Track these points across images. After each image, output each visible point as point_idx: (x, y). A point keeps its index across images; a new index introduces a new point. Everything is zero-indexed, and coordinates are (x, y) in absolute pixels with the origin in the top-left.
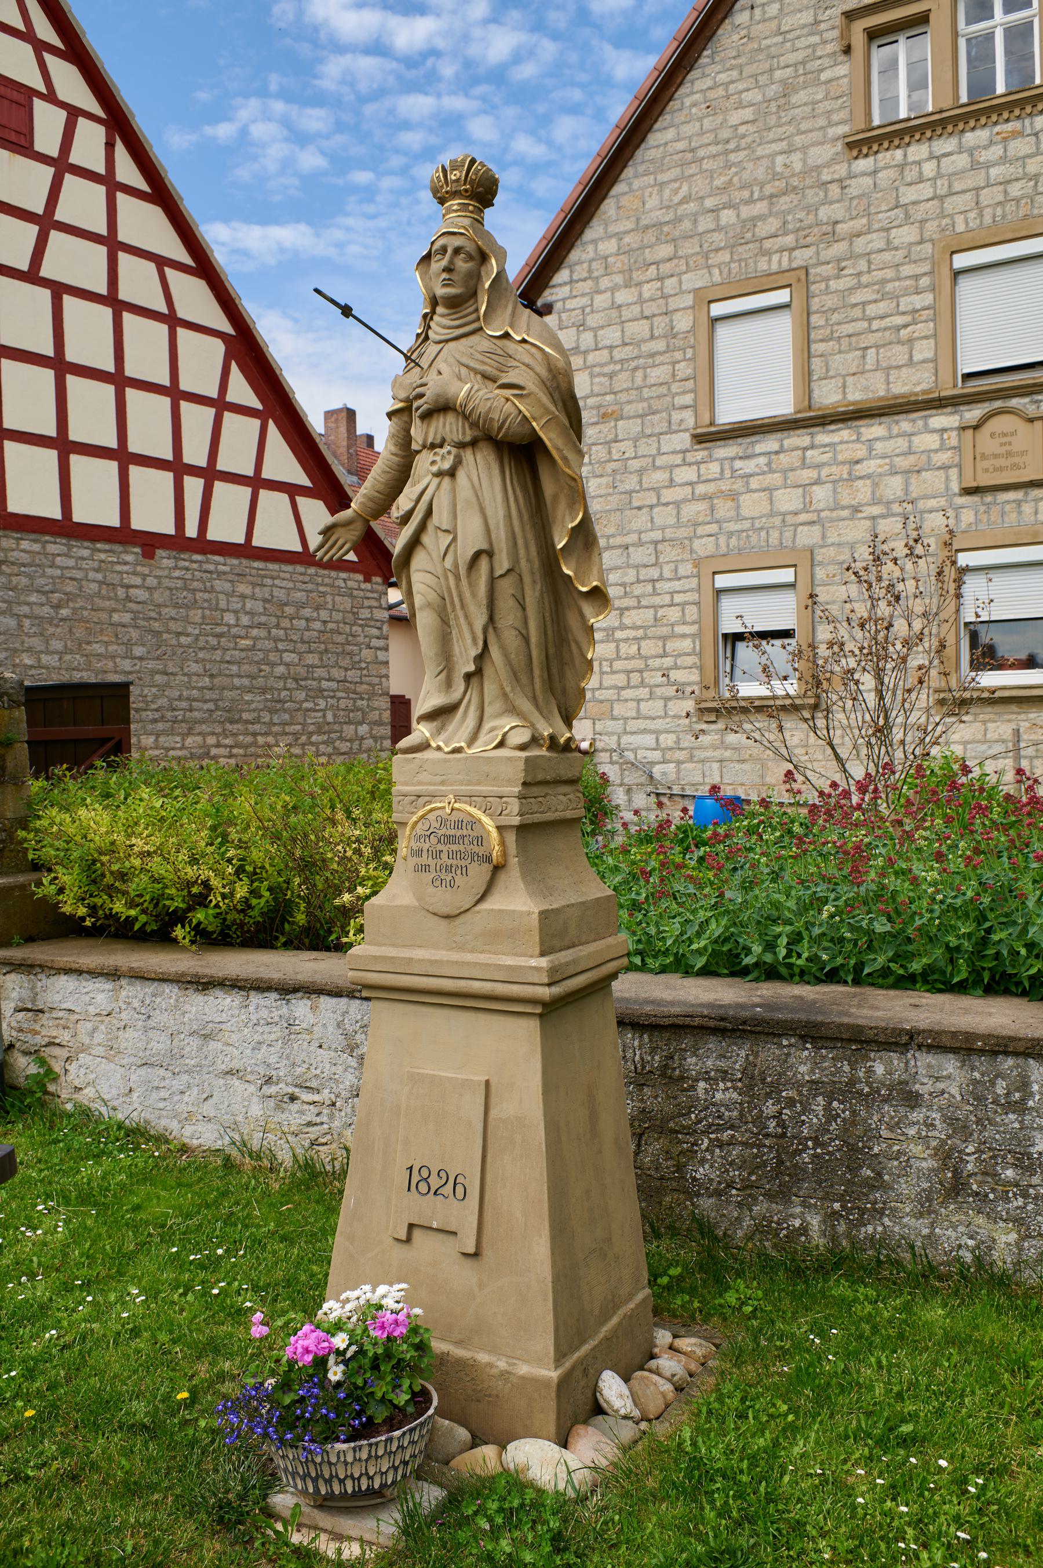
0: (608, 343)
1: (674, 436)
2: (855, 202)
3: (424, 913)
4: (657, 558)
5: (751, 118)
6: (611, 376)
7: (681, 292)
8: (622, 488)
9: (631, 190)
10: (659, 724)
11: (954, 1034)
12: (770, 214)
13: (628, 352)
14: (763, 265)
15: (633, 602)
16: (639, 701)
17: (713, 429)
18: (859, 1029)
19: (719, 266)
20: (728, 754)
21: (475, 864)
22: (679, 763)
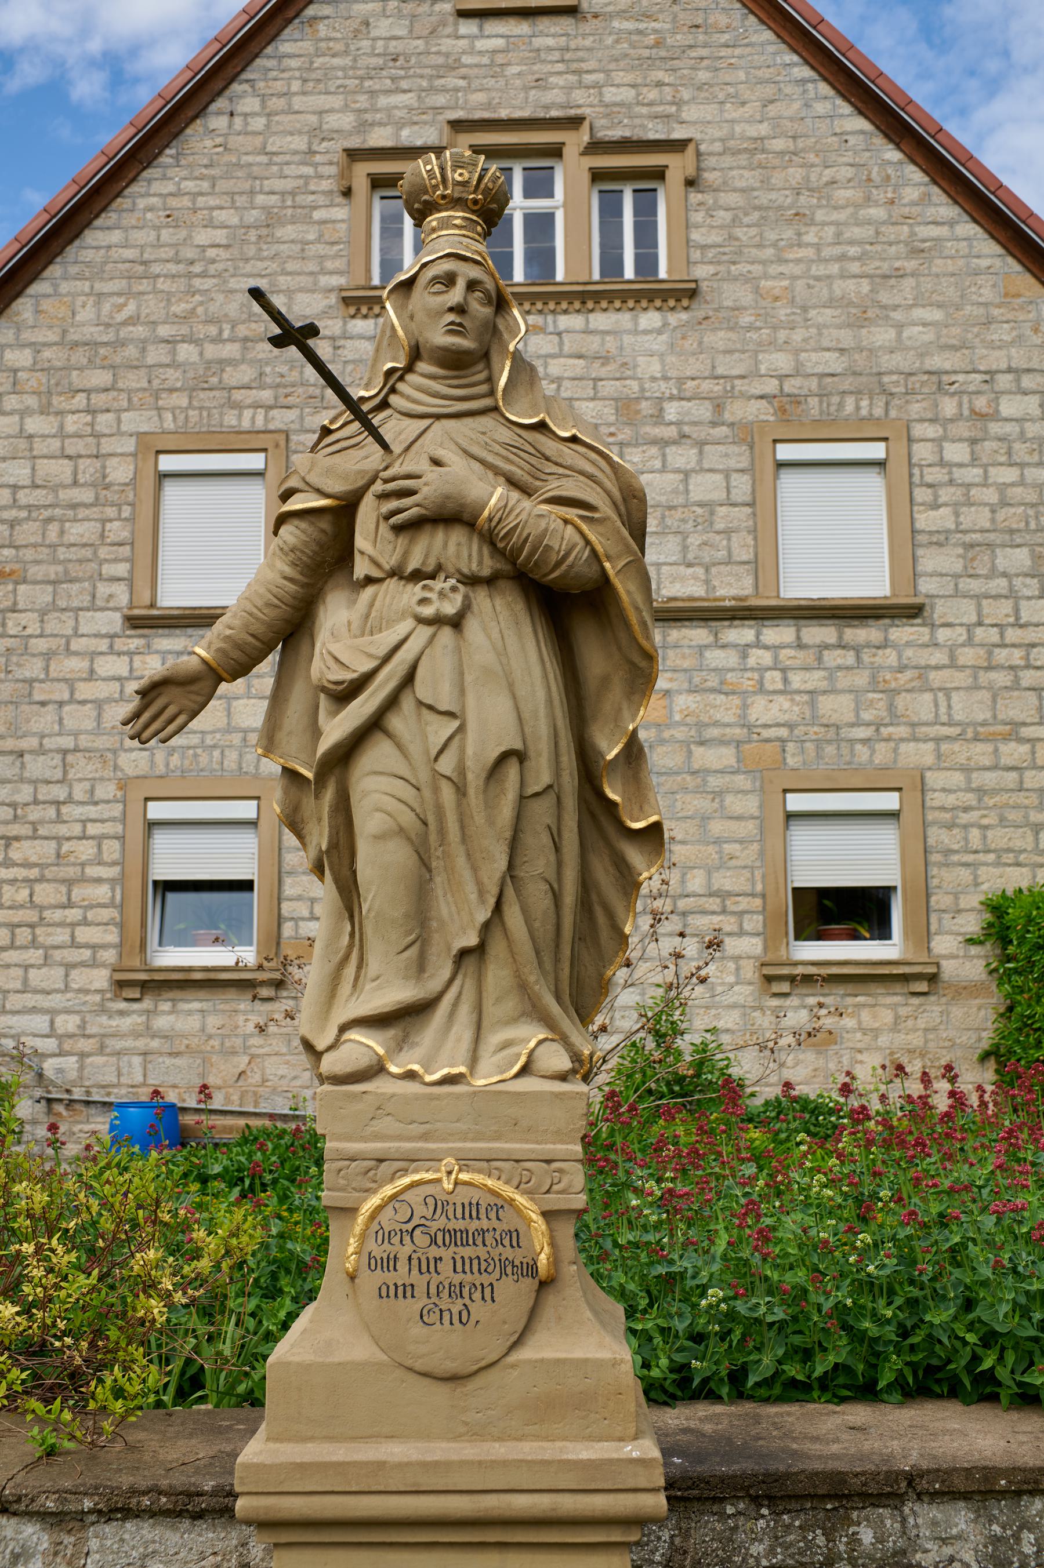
0: (12, 481)
1: (99, 614)
2: (350, 368)
3: (400, 1373)
4: (65, 773)
5: (224, 242)
6: (12, 524)
7: (119, 433)
8: (19, 674)
9: (56, 294)
10: (56, 1001)
11: (968, 1472)
12: (243, 361)
13: (39, 496)
14: (230, 419)
15: (25, 830)
16: (27, 968)
17: (155, 612)
18: (838, 1478)
19: (173, 410)
20: (155, 1044)
21: (508, 1281)
22: (82, 1055)
